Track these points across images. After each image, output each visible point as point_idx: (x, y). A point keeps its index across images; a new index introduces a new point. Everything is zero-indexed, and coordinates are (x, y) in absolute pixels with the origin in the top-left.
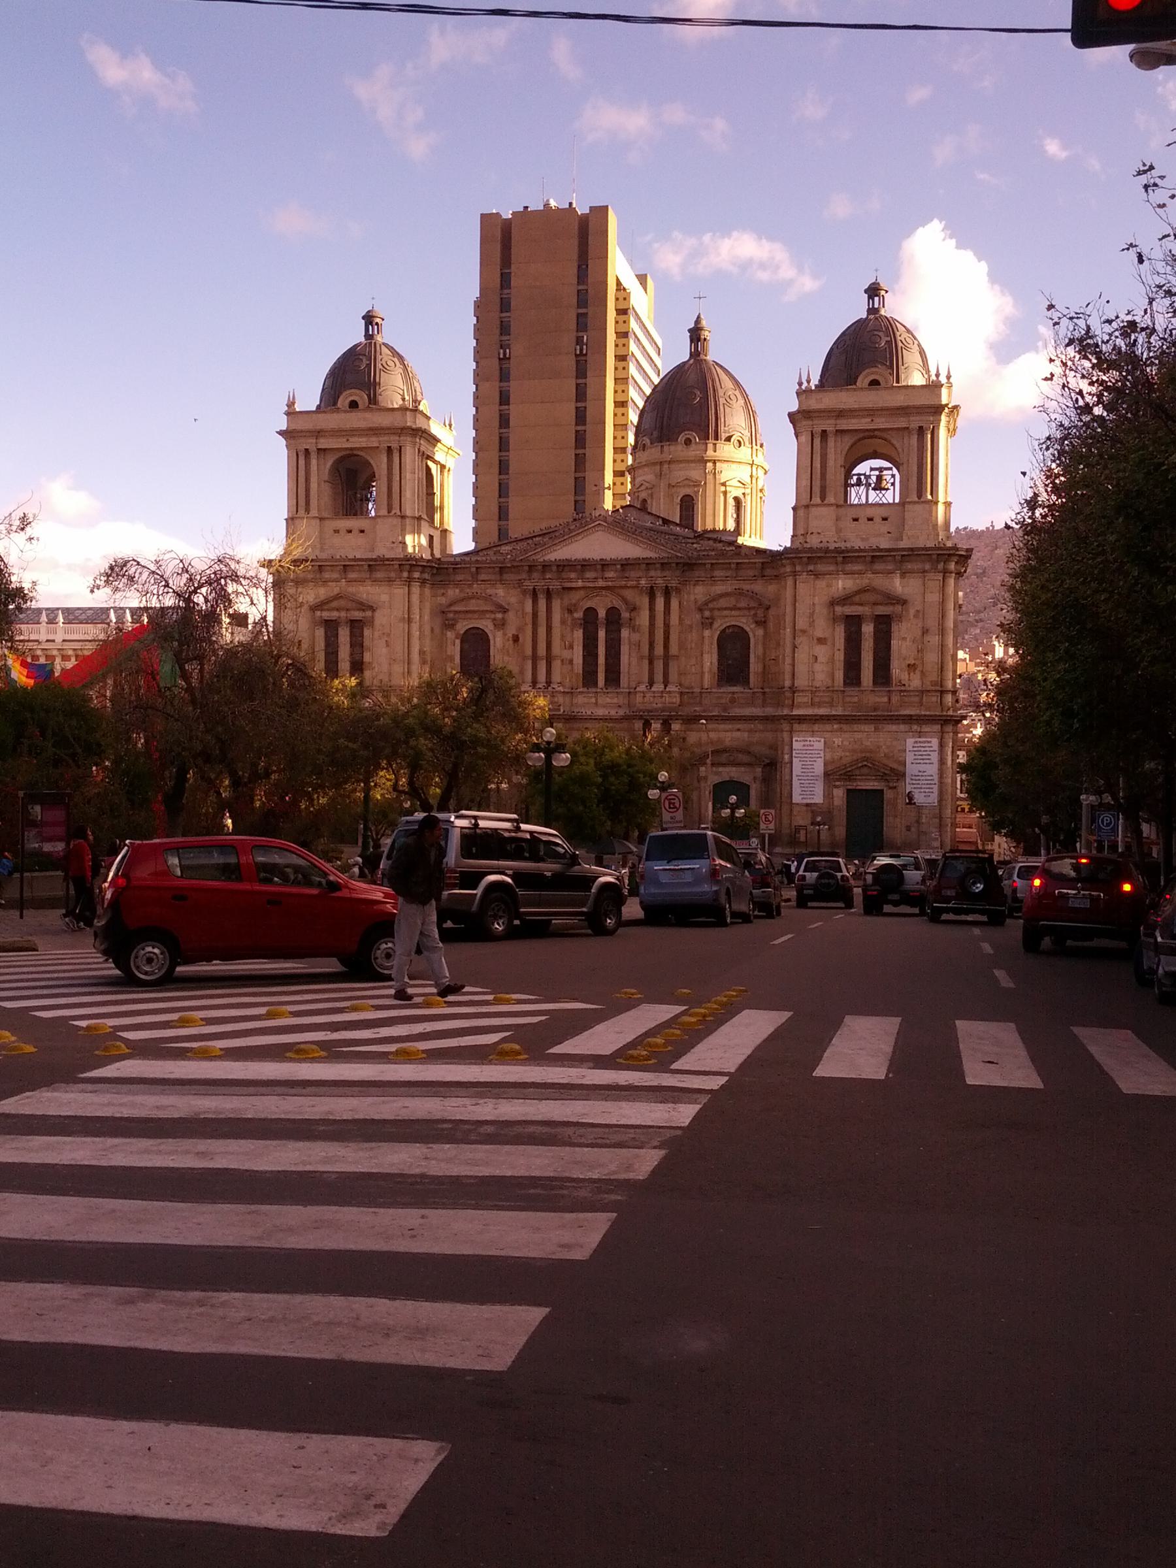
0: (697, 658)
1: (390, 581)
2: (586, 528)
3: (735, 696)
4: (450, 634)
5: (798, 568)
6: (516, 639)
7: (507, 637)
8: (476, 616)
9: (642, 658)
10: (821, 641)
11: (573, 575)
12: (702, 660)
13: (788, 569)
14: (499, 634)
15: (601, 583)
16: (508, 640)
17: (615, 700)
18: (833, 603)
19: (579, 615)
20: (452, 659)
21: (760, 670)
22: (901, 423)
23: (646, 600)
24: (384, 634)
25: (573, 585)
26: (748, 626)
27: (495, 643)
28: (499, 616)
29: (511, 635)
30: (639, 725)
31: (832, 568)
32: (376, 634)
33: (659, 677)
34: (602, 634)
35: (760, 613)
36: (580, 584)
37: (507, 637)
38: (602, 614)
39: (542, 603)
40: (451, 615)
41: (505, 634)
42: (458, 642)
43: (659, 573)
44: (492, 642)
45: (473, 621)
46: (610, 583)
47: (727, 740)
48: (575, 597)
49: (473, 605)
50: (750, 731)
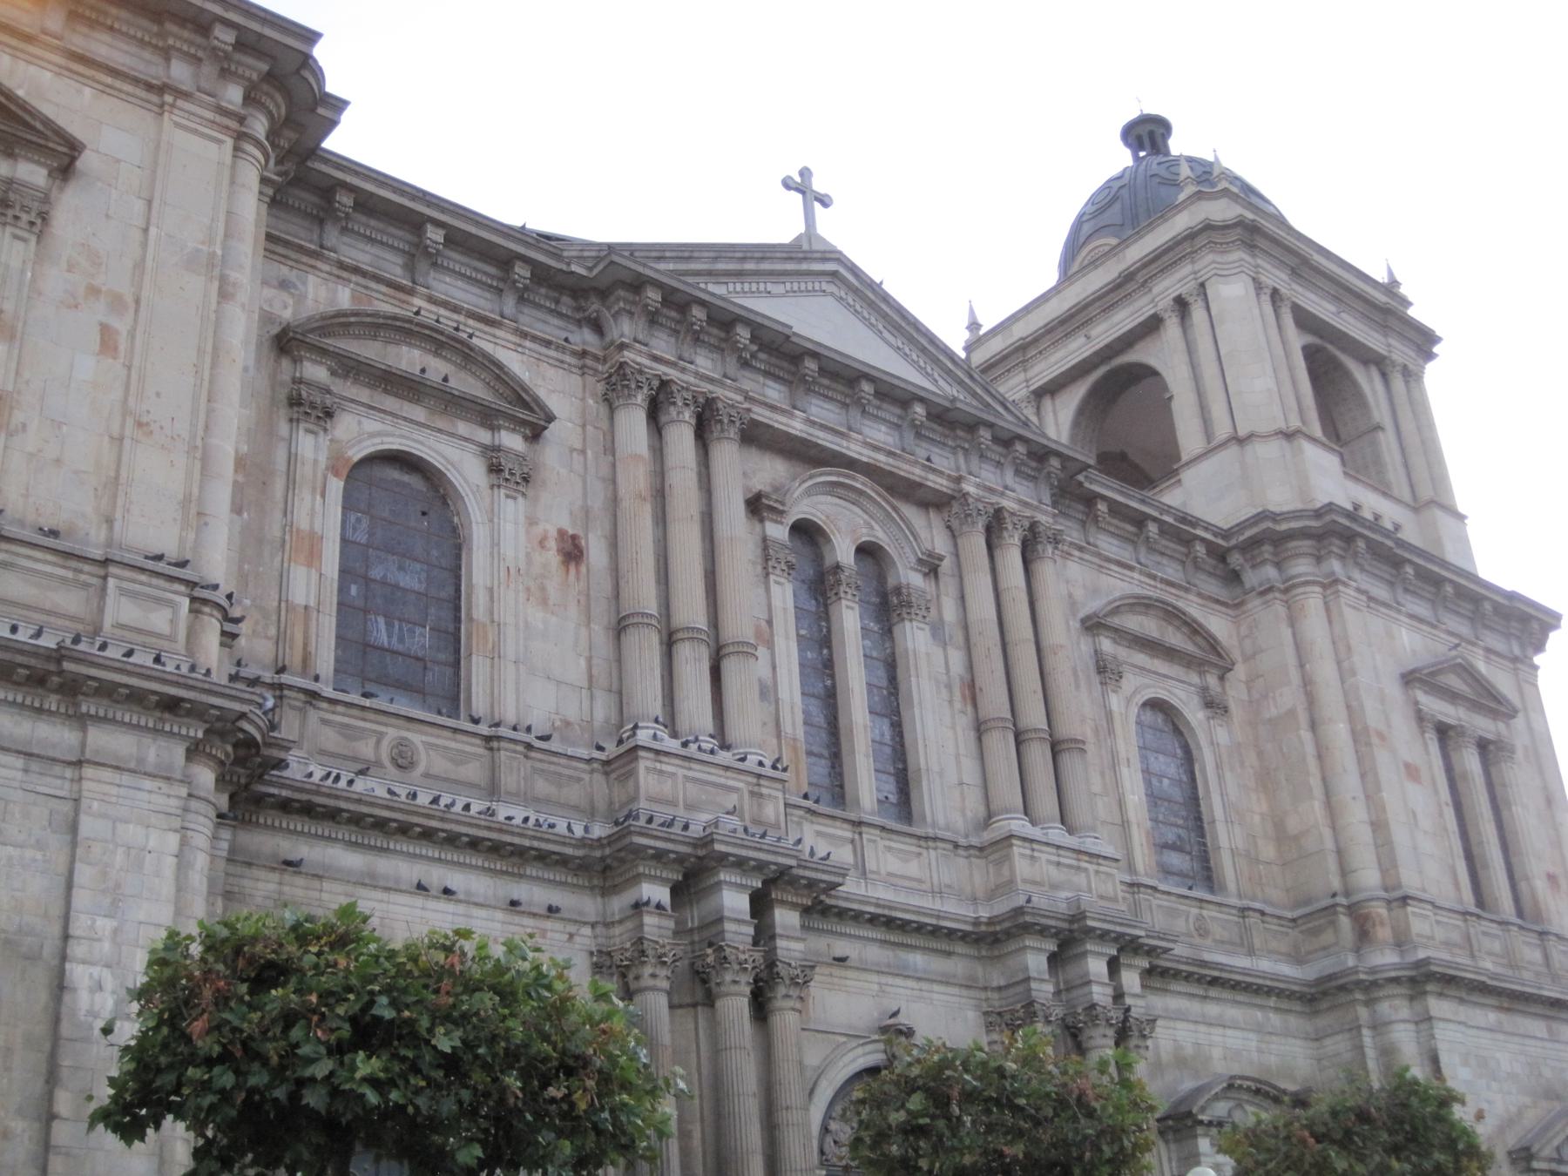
0: (1103, 774)
1: (160, 91)
2: (804, 266)
3: (1205, 913)
4: (310, 447)
5: (1336, 565)
6: (572, 552)
7: (538, 530)
8: (418, 413)
9: (980, 729)
10: (1412, 772)
11: (774, 392)
12: (1117, 783)
13: (1302, 567)
14: (512, 510)
15: (854, 450)
16: (542, 543)
17: (913, 869)
18: (1409, 679)
19: (778, 532)
20: (311, 549)
21: (1240, 843)
22: (1372, 339)
23: (975, 542)
24: (94, 291)
25: (779, 422)
26: (1194, 714)
27: (495, 544)
28: (512, 441)
29: (553, 533)
30: (1035, 961)
31: (1381, 592)
32: (55, 281)
33: (1046, 801)
34: (850, 619)
35: (1212, 680)
36: (796, 426)
37: (538, 530)
38: (843, 551)
39: (681, 438)
40: (316, 372)
41: (532, 522)
42: (336, 486)
43: (1009, 477)
44: (479, 535)
45: (406, 428)
46: (882, 457)
47: (1217, 1053)
48: (768, 471)
49: (409, 358)
50: (1259, 1029)
